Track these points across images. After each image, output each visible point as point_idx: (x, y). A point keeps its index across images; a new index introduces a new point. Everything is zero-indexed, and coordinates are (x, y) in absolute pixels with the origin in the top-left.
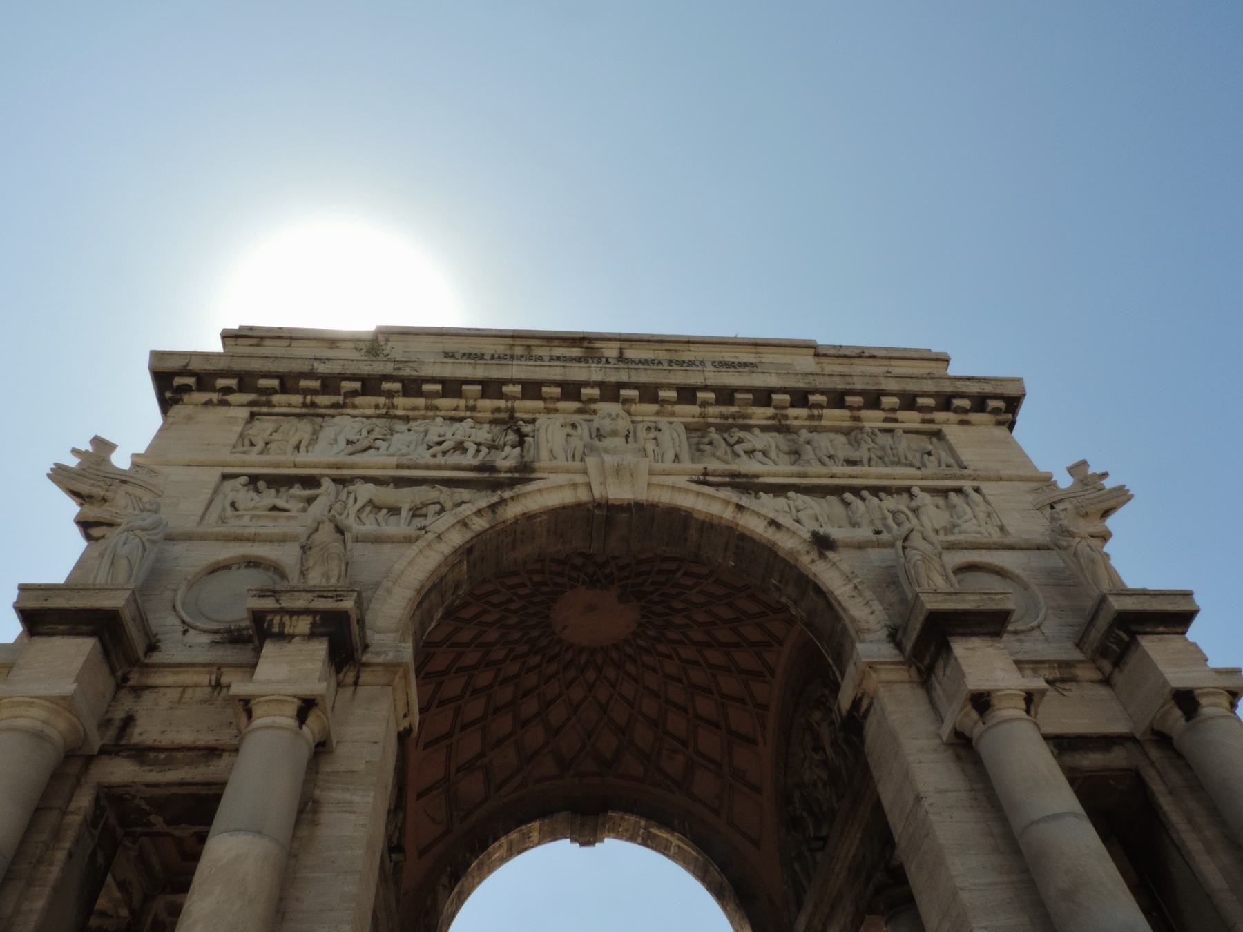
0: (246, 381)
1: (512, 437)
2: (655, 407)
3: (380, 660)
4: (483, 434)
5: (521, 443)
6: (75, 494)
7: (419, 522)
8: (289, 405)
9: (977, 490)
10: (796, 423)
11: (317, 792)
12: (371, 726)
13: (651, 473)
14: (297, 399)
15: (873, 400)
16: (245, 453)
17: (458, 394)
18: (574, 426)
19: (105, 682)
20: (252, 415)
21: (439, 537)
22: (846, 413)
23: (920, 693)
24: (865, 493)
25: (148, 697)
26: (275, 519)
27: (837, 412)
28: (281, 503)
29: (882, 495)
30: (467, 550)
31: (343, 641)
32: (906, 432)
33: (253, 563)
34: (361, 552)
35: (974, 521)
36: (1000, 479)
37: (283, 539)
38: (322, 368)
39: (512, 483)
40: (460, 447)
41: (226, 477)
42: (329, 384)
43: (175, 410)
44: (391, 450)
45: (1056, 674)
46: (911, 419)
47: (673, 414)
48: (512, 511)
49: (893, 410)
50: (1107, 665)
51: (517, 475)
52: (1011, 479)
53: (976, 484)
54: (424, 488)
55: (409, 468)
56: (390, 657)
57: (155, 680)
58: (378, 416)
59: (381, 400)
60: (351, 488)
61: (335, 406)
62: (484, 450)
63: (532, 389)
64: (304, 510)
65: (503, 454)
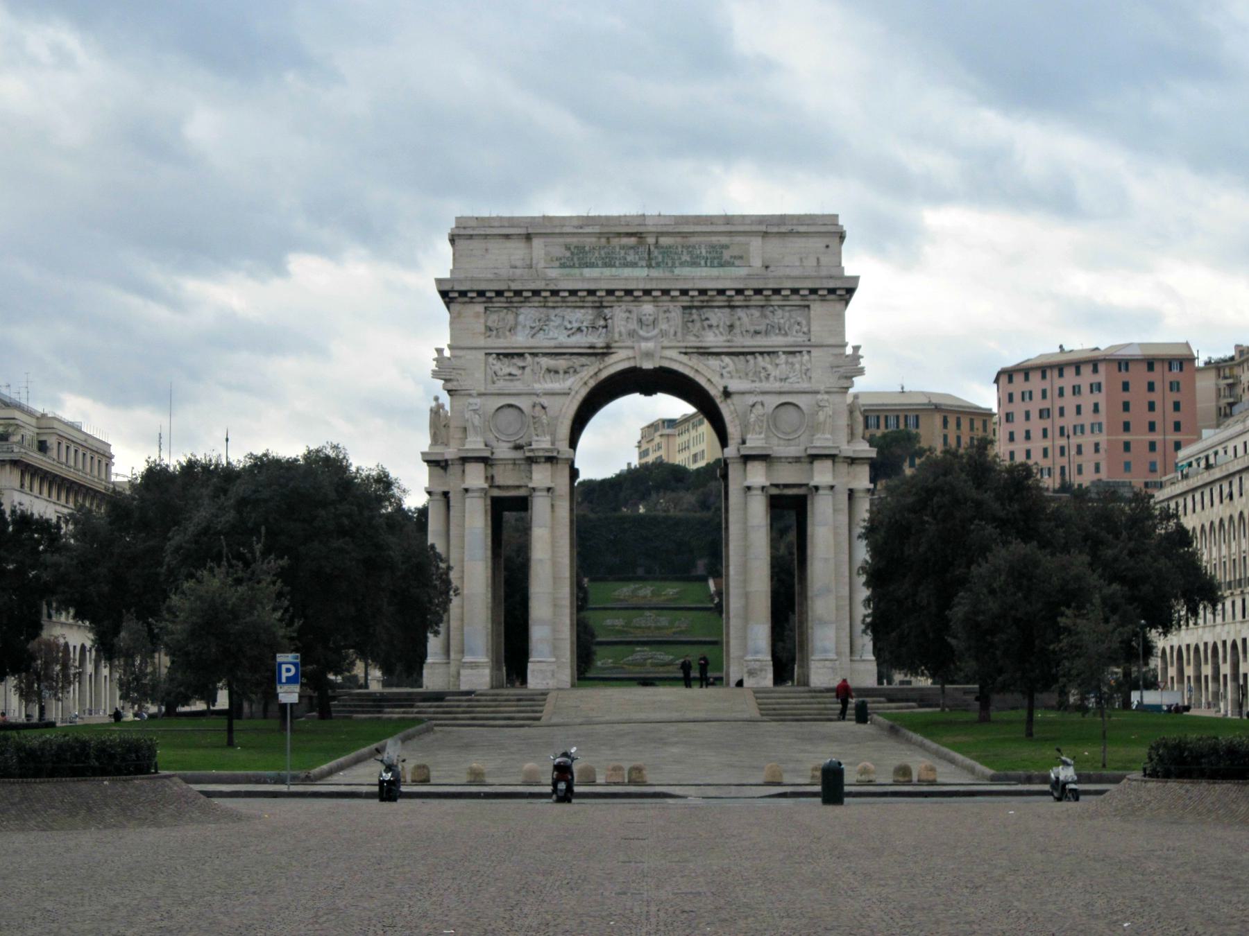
0: (481, 293)
1: (602, 323)
5: (606, 327)
10: (737, 304)
13: (663, 348)
14: (502, 299)
15: (777, 291)
18: (630, 312)
20: (486, 308)
27: (758, 297)
38: (515, 286)
39: (604, 354)
42: (518, 293)
43: (452, 305)
46: (795, 300)
48: (604, 375)
56: (566, 456)
60: (537, 359)
63: (610, 292)
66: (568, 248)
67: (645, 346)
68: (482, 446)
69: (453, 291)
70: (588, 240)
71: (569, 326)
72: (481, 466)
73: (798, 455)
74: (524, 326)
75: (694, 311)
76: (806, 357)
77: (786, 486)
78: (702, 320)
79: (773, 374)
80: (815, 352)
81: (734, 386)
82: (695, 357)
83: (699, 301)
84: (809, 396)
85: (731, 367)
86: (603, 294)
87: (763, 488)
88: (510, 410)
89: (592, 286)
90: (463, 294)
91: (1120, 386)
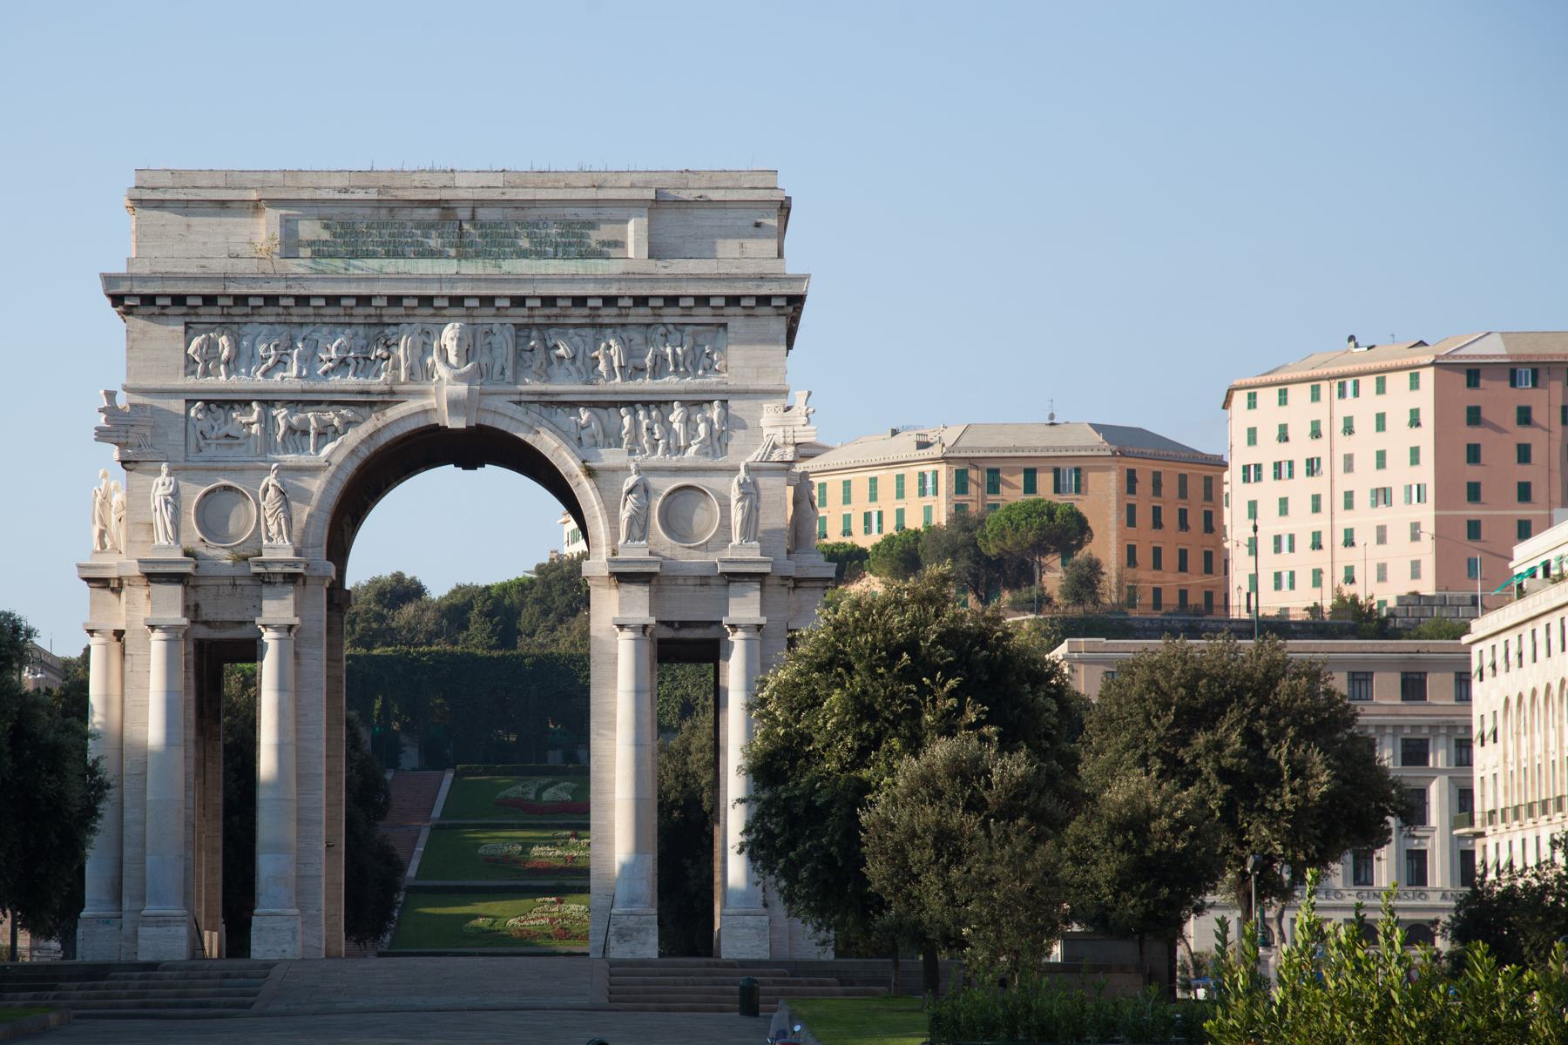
0: (179, 300)
2: (492, 311)
10: (607, 321)
14: (217, 310)
15: (672, 301)
22: (649, 311)
24: (638, 406)
26: (231, 445)
27: (642, 310)
38: (235, 289)
42: (241, 300)
46: (704, 315)
49: (690, 308)
51: (387, 398)
56: (321, 573)
57: (201, 582)
59: (281, 310)
61: (247, 315)
62: (362, 362)
63: (395, 300)
68: (179, 556)
70: (359, 211)
72: (178, 590)
75: (534, 333)
77: (684, 624)
78: (547, 349)
83: (541, 319)
86: (384, 303)
87: (645, 627)
90: (148, 300)
91: (1463, 416)
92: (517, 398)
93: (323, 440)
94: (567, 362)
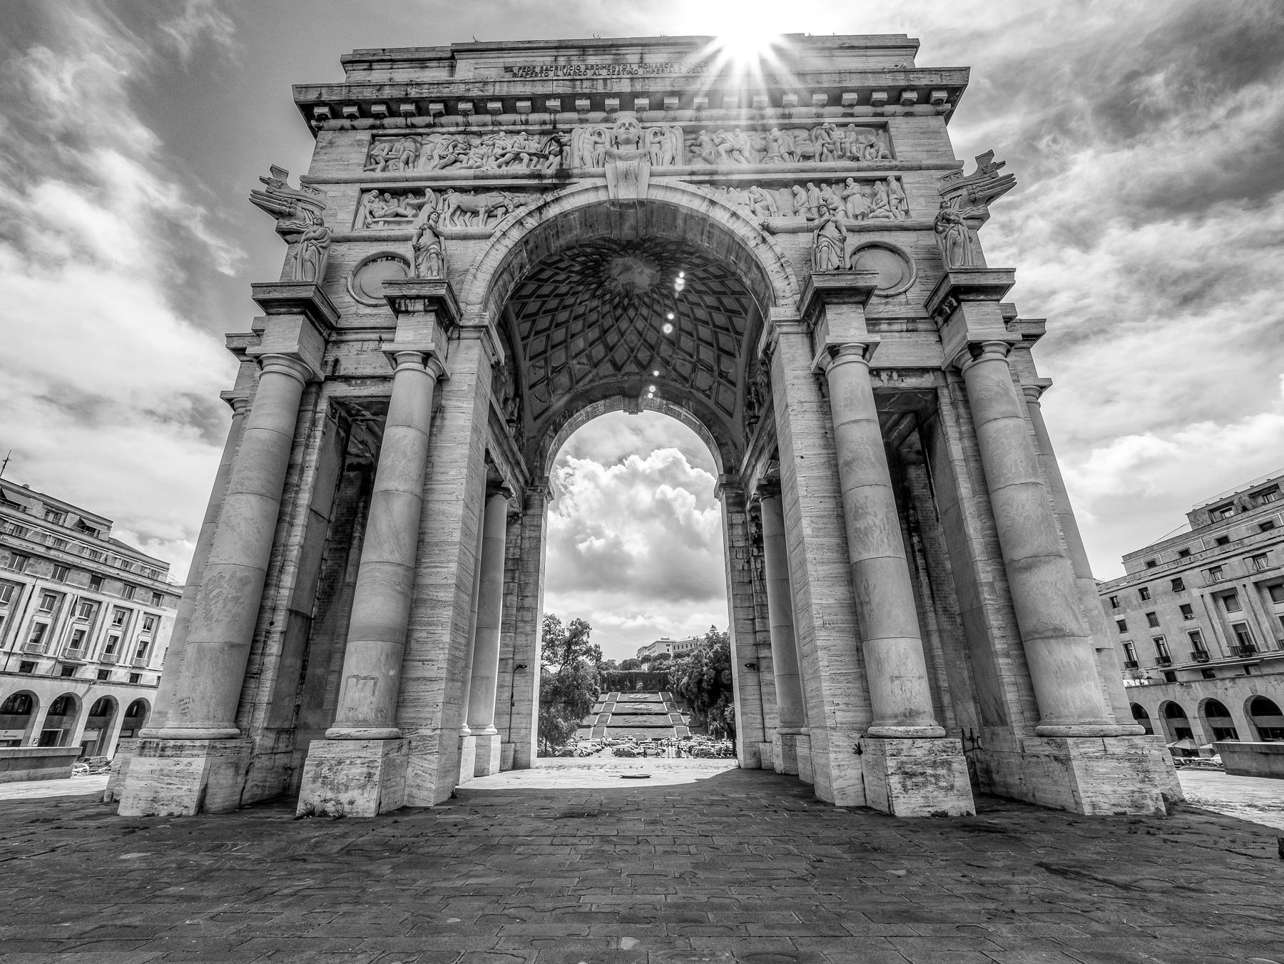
0: (364, 109)
1: (555, 147)
3: (470, 324)
4: (534, 145)
5: (561, 152)
6: (272, 212)
7: (493, 222)
8: (397, 127)
9: (898, 179)
11: (443, 402)
12: (470, 364)
13: (652, 175)
16: (373, 170)
17: (514, 110)
18: (599, 134)
19: (316, 341)
20: (374, 136)
21: (504, 234)
23: (806, 341)
24: (810, 185)
25: (344, 347)
26: (399, 223)
28: (401, 211)
29: (823, 185)
30: (525, 241)
31: (444, 313)
32: (857, 125)
33: (391, 257)
34: (453, 247)
35: (887, 207)
36: (920, 169)
37: (406, 239)
38: (413, 92)
39: (555, 187)
40: (517, 158)
41: (363, 191)
42: (421, 107)
44: (471, 162)
45: (904, 327)
47: (675, 119)
48: (553, 211)
49: (851, 106)
50: (940, 320)
51: (555, 181)
52: (928, 168)
53: (898, 173)
54: (494, 194)
55: (482, 178)
56: (476, 322)
58: (460, 133)
59: (460, 119)
64: (415, 216)
65: (548, 163)
66: (508, 69)
67: (621, 165)
69: (321, 103)
71: (501, 152)
73: (912, 315)
74: (431, 158)
76: (894, 184)
79: (842, 207)
80: (907, 177)
81: (777, 222)
82: (706, 190)
84: (913, 235)
85: (769, 198)
88: (390, 263)
89: (540, 89)
92: (688, 178)
93: (491, 220)
94: (736, 154)
